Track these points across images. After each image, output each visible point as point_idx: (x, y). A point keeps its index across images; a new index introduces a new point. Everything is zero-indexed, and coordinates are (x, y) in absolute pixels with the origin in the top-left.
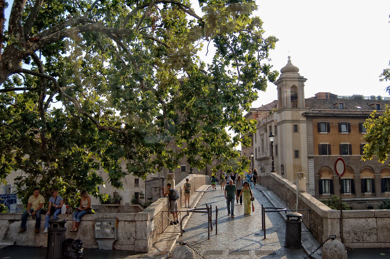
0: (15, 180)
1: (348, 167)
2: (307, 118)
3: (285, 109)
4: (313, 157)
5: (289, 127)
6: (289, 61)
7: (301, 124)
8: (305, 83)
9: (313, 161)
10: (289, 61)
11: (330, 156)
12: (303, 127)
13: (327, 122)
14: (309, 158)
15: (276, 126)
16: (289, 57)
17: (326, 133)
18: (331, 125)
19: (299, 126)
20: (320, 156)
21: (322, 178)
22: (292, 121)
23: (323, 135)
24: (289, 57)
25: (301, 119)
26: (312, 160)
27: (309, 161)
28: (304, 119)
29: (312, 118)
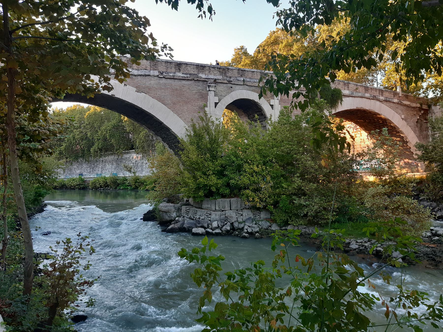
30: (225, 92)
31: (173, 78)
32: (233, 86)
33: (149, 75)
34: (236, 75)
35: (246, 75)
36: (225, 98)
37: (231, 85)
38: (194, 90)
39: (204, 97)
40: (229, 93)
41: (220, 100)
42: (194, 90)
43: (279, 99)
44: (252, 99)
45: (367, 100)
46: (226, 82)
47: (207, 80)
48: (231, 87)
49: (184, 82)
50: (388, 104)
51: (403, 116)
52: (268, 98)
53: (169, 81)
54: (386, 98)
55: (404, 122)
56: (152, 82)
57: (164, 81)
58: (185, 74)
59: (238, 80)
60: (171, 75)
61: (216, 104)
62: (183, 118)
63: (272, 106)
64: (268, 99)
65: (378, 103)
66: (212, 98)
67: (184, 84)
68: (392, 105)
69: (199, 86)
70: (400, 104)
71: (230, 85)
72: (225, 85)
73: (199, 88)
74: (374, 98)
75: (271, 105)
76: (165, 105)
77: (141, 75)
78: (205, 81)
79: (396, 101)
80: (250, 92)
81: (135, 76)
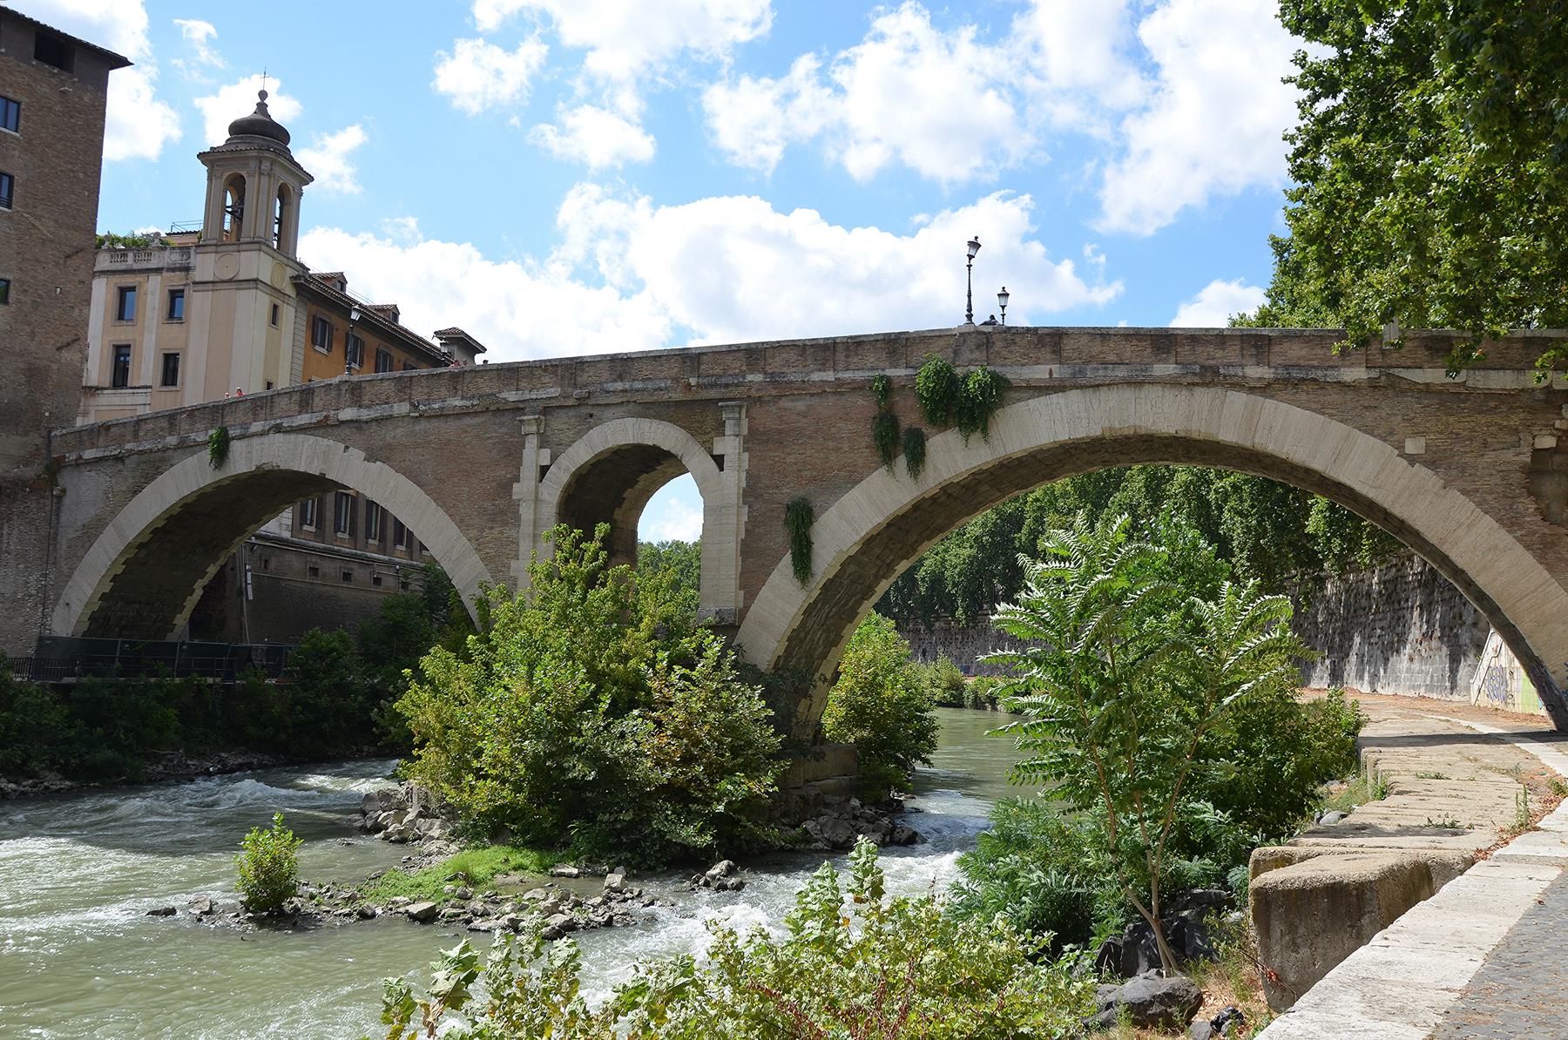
2: (297, 295)
3: (263, 247)
5: (263, 302)
6: (262, 107)
8: (304, 188)
10: (262, 107)
12: (288, 313)
15: (175, 295)
16: (263, 95)
17: (324, 351)
18: (335, 333)
19: (280, 310)
22: (275, 290)
23: (318, 356)
24: (263, 95)
28: (290, 291)
29: (309, 299)
30: (570, 434)
31: (442, 415)
32: (595, 412)
33: (391, 417)
34: (606, 375)
35: (633, 372)
36: (570, 449)
37: (590, 410)
38: (489, 438)
39: (513, 454)
40: (580, 434)
41: (554, 458)
42: (489, 438)
43: (746, 432)
44: (650, 443)
45: (1169, 394)
46: (570, 402)
47: (522, 406)
48: (591, 416)
49: (468, 420)
50: (1304, 397)
51: (1413, 446)
52: (706, 433)
53: (435, 423)
54: (1286, 367)
55: (1421, 471)
56: (400, 432)
57: (423, 425)
58: (466, 399)
59: (608, 392)
60: (436, 406)
61: (544, 470)
62: (458, 518)
63: (719, 460)
64: (706, 438)
65: (1238, 399)
66: (533, 455)
67: (468, 426)
68: (1333, 397)
69: (502, 425)
70: (1386, 385)
71: (584, 411)
72: (572, 413)
73: (504, 430)
74: (1210, 377)
75: (713, 457)
76: (420, 486)
77: (376, 420)
78: (518, 409)
79: (1356, 373)
80: (645, 424)
81: (367, 422)
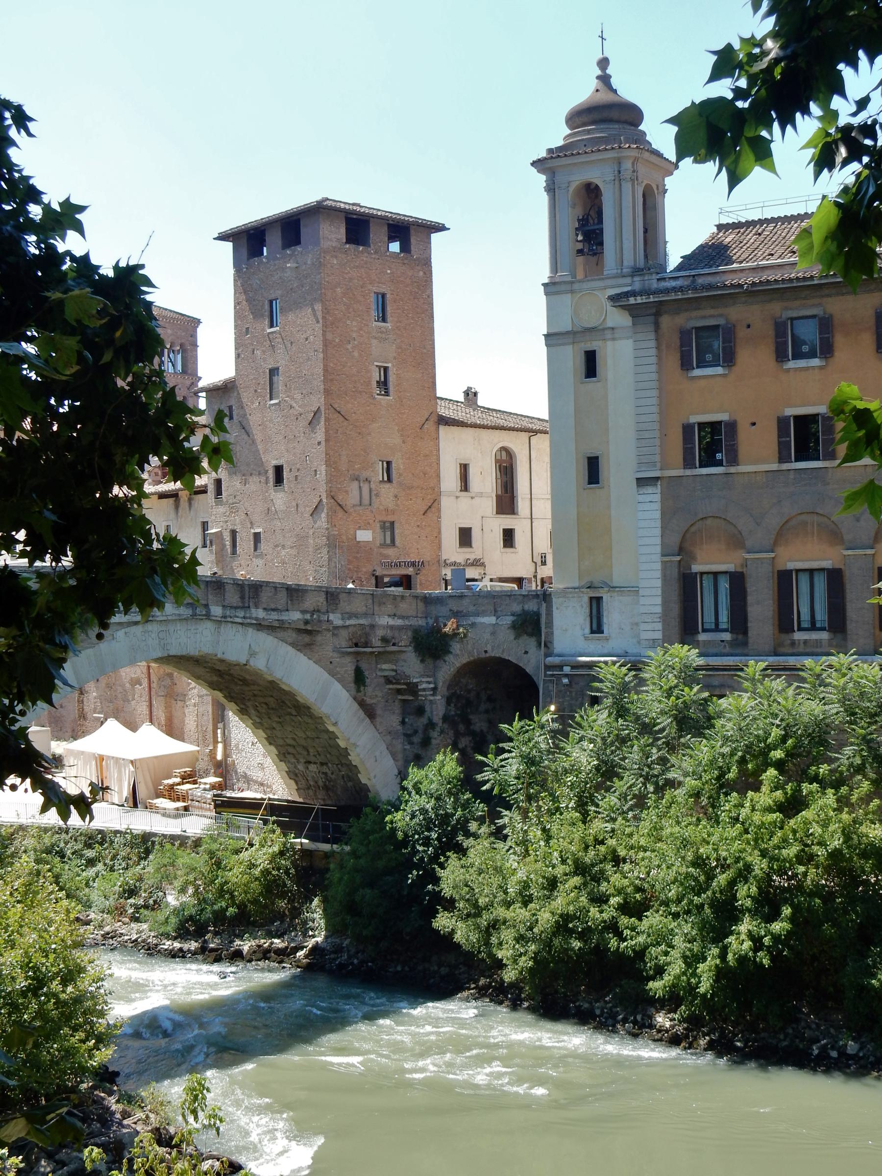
0: (762, 671)
1: (816, 518)
4: (657, 478)
6: (605, 79)
7: (609, 343)
9: (657, 498)
10: (605, 79)
11: (732, 470)
13: (721, 321)
14: (642, 482)
16: (604, 63)
20: (688, 472)
21: (696, 568)
23: (702, 383)
24: (604, 63)
25: (610, 324)
26: (650, 490)
27: (641, 498)
